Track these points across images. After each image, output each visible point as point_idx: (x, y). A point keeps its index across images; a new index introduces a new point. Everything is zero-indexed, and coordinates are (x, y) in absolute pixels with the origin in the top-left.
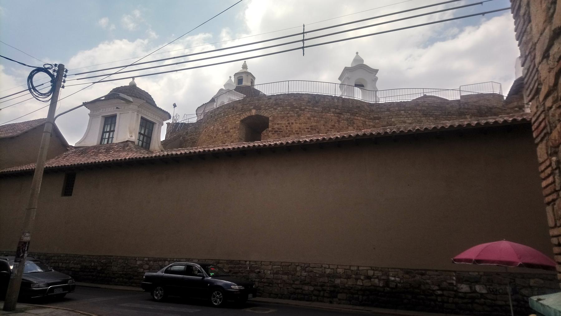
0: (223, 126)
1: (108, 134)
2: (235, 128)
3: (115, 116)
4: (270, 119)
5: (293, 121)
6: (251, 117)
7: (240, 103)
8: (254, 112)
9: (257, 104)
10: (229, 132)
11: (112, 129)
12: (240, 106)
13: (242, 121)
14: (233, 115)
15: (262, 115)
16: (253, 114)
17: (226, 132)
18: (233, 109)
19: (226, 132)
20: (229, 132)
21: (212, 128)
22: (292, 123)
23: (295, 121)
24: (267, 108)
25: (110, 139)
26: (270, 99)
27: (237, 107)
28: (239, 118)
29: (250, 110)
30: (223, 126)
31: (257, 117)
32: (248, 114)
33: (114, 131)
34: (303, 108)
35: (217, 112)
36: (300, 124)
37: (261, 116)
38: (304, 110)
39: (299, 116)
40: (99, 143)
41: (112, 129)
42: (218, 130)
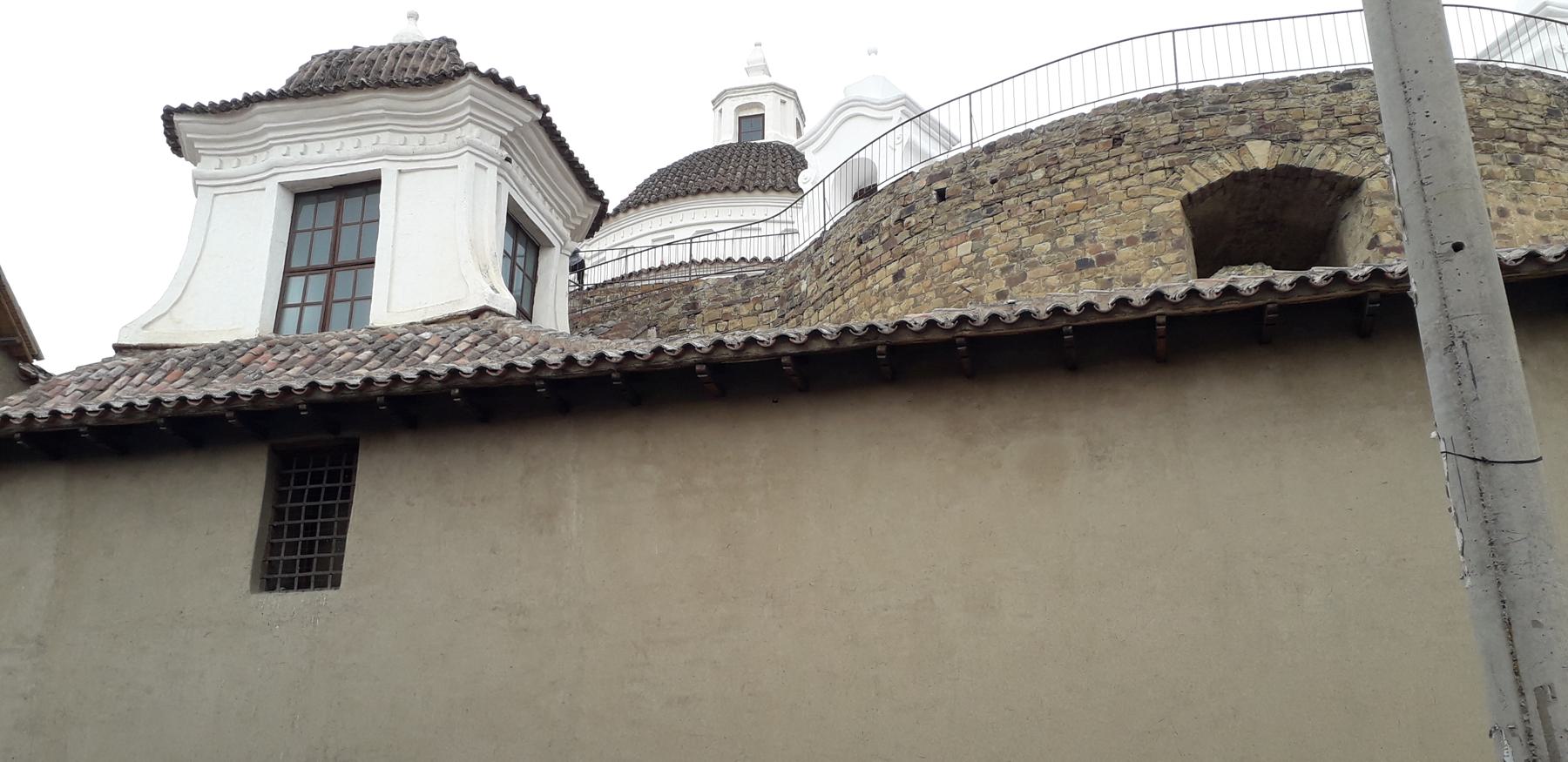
0: (1053, 236)
1: (318, 283)
2: (1150, 236)
3: (370, 185)
4: (1375, 185)
5: (1503, 202)
6: (1239, 179)
7: (1158, 109)
8: (1261, 155)
9: (1269, 117)
10: (1106, 259)
11: (346, 255)
12: (1164, 128)
13: (1189, 202)
14: (1122, 171)
15: (1321, 166)
16: (1262, 165)
17: (1083, 264)
18: (1118, 141)
19: (1083, 264)
20: (1106, 259)
21: (965, 248)
22: (1503, 213)
23: (1515, 199)
24: (1335, 132)
25: (339, 312)
26: (1349, 87)
27: (1142, 132)
28: (1174, 186)
29: (1237, 145)
30: (1061, 233)
31: (1287, 176)
32: (1224, 165)
33: (372, 263)
34: (1534, 137)
35: (993, 170)
36: (1539, 216)
37: (1308, 171)
38: (1540, 149)
39: (1527, 177)
40: (268, 331)
41: (346, 255)
42: (1016, 255)
